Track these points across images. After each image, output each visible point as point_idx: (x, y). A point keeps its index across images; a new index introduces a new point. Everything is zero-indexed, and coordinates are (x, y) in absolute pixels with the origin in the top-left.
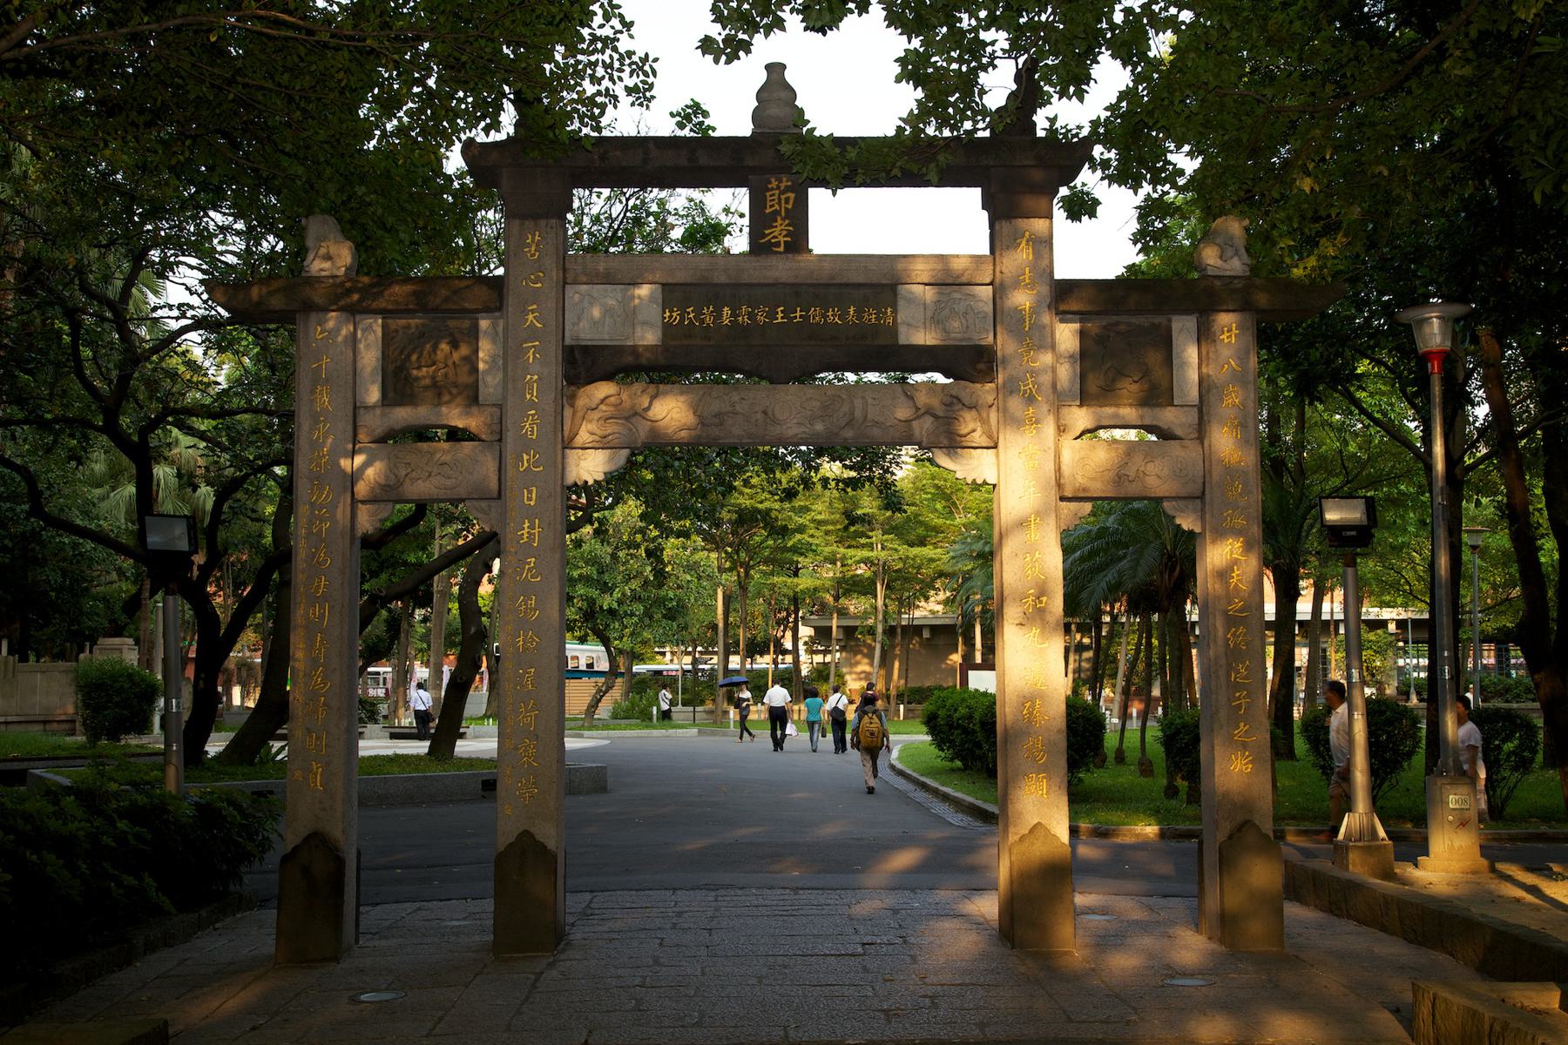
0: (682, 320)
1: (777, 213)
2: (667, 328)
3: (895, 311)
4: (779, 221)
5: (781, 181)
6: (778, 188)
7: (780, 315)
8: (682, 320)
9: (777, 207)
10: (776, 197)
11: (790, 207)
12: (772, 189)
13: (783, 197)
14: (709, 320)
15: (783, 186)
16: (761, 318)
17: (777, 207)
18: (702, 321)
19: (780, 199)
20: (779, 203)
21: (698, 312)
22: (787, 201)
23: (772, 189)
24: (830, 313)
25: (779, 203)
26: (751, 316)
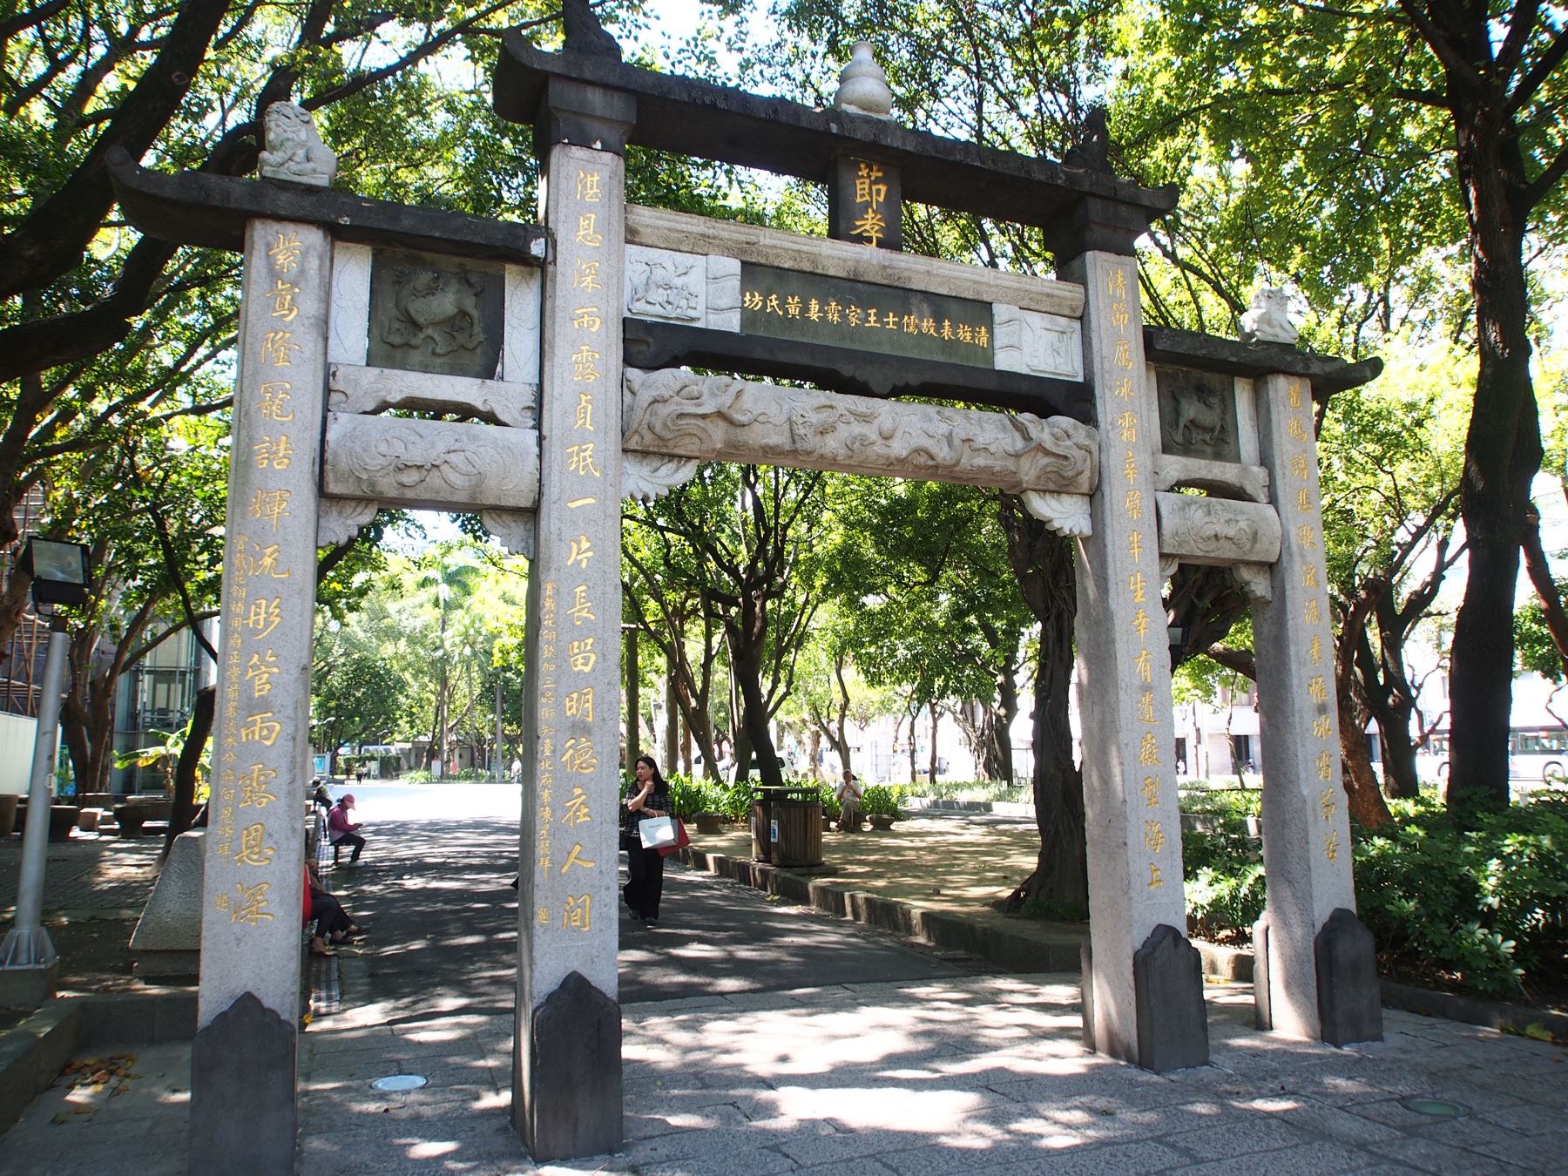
0: (765, 306)
1: (869, 204)
2: (749, 317)
3: (991, 331)
4: (871, 214)
5: (871, 170)
6: (869, 177)
7: (872, 318)
8: (765, 306)
9: (868, 198)
10: (867, 187)
11: (881, 199)
12: (863, 177)
13: (874, 188)
14: (793, 310)
15: (874, 175)
16: (854, 321)
17: (868, 198)
18: (786, 312)
19: (870, 189)
20: (870, 194)
21: (783, 304)
23: (863, 177)
24: (925, 324)
25: (870, 194)
26: (843, 316)
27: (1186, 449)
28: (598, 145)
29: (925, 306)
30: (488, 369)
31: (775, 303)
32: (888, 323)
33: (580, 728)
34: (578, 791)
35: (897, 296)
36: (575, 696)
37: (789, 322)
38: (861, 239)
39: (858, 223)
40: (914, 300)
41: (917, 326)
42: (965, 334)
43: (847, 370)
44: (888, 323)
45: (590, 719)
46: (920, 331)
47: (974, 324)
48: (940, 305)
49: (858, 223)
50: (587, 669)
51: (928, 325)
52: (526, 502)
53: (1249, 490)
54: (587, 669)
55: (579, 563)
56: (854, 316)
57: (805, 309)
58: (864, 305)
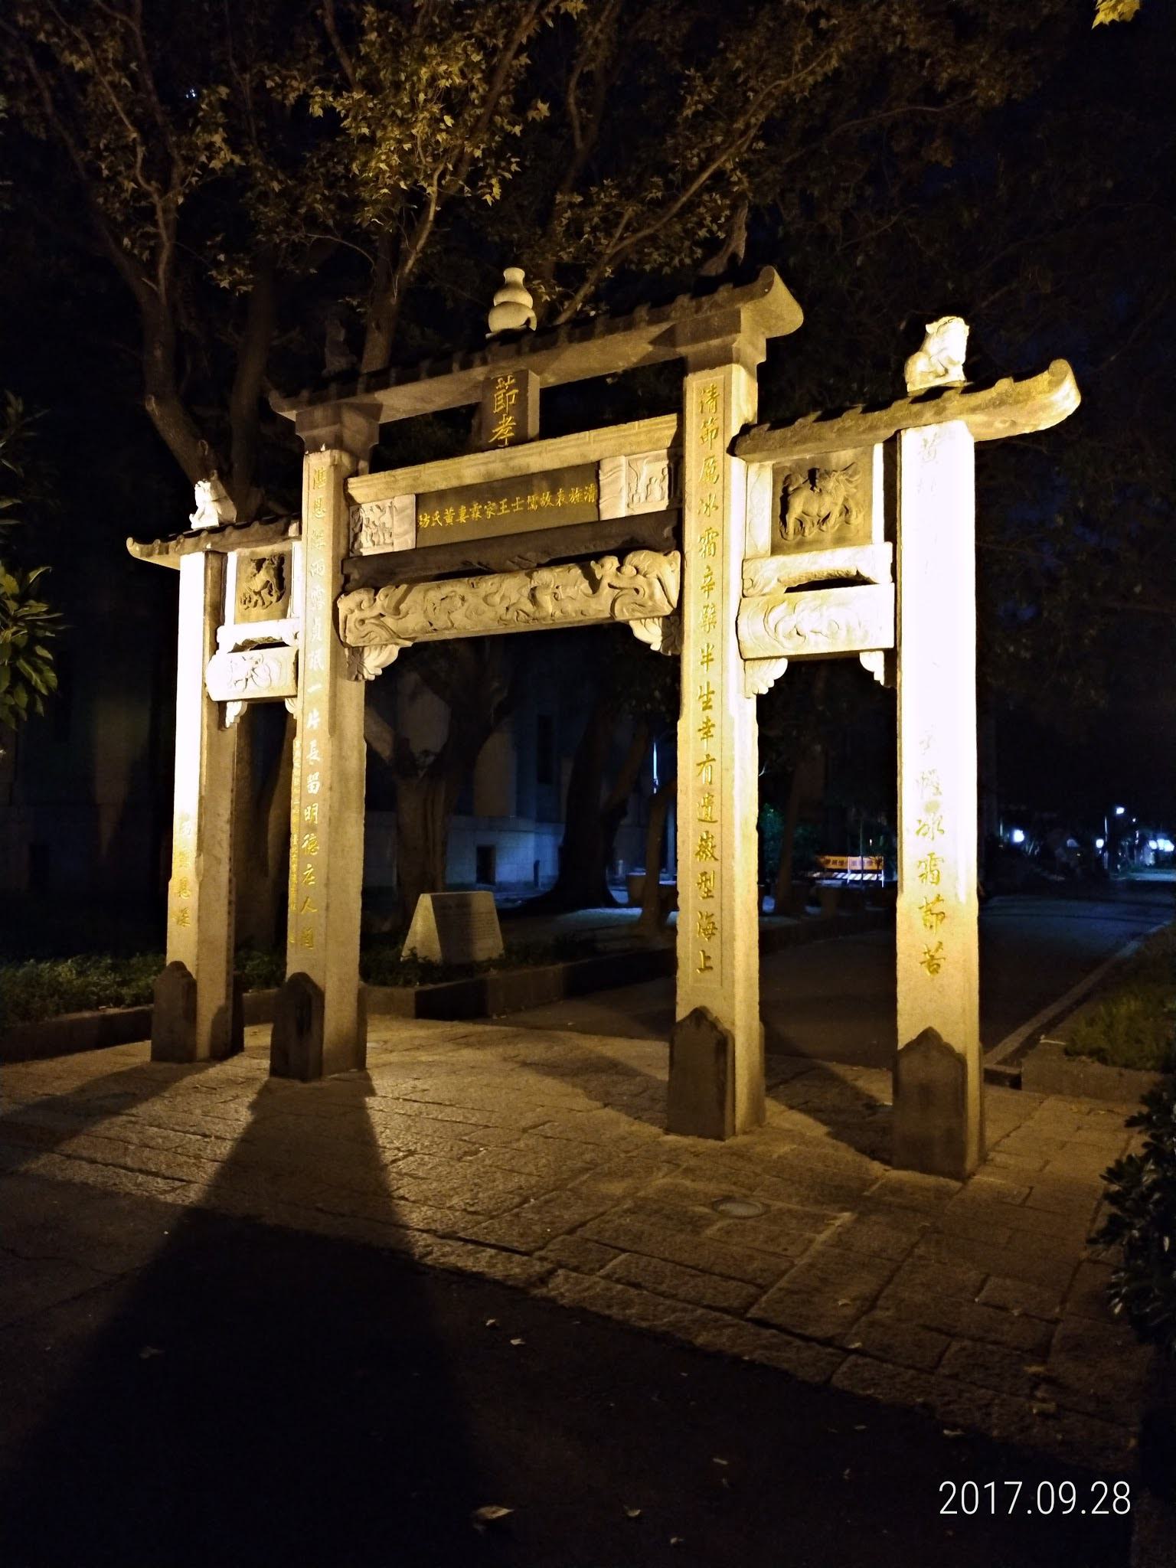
7: (503, 508)
14: (449, 520)
16: (489, 513)
18: (444, 522)
22: (510, 400)
26: (483, 512)
27: (801, 546)
28: (323, 448)
29: (544, 484)
30: (284, 614)
31: (437, 519)
32: (515, 507)
33: (311, 828)
34: (309, 866)
35: (523, 483)
36: (309, 808)
37: (447, 529)
38: (496, 445)
39: (497, 430)
40: (535, 482)
41: (537, 503)
42: (575, 496)
43: (474, 558)
44: (515, 507)
45: (316, 822)
46: (539, 506)
47: (582, 484)
48: (554, 479)
49: (497, 430)
50: (315, 792)
51: (546, 498)
52: (293, 693)
53: (866, 573)
54: (315, 792)
55: (312, 726)
56: (490, 509)
57: (457, 516)
58: (496, 498)
